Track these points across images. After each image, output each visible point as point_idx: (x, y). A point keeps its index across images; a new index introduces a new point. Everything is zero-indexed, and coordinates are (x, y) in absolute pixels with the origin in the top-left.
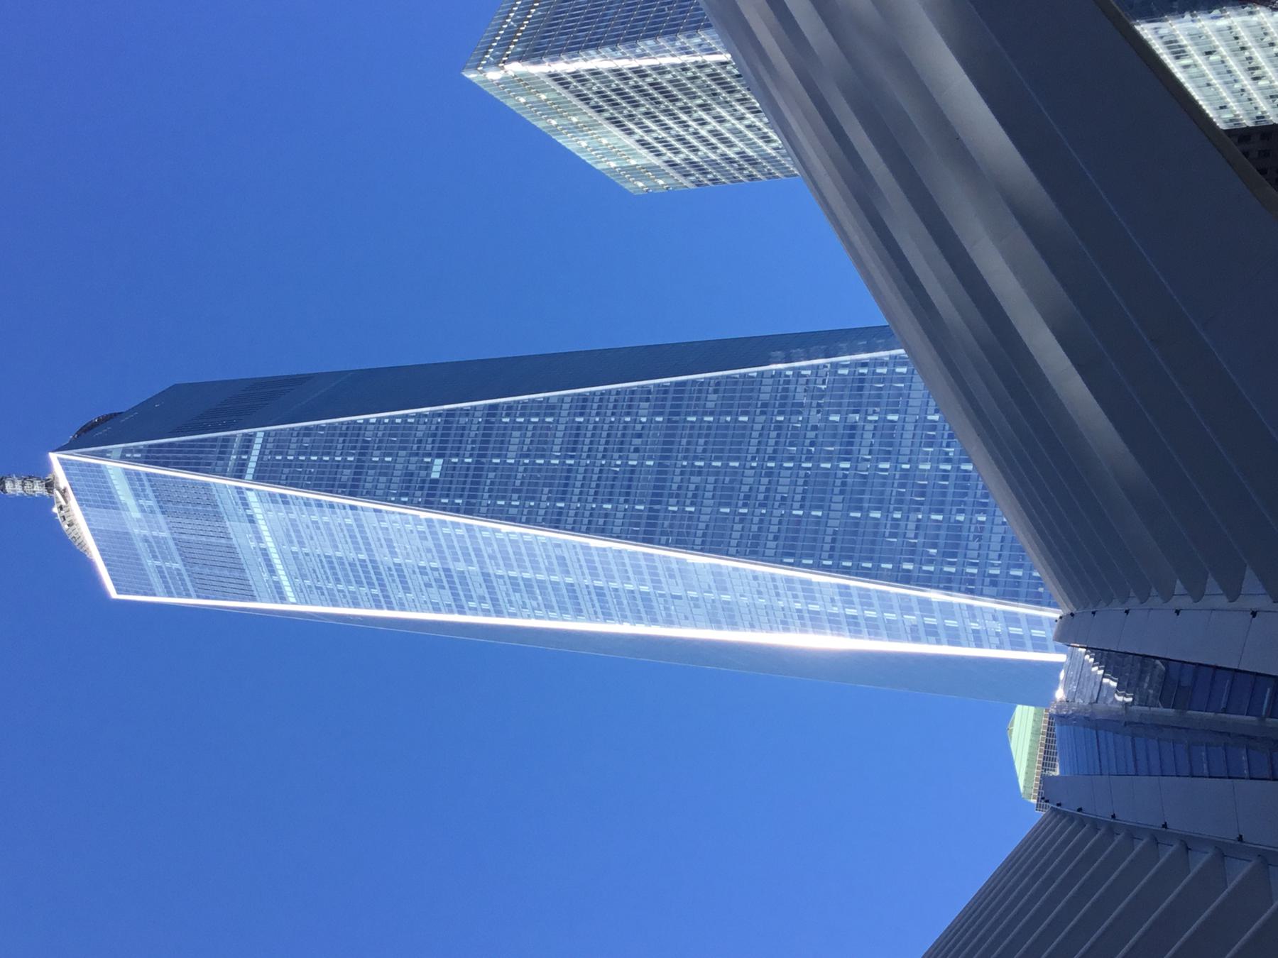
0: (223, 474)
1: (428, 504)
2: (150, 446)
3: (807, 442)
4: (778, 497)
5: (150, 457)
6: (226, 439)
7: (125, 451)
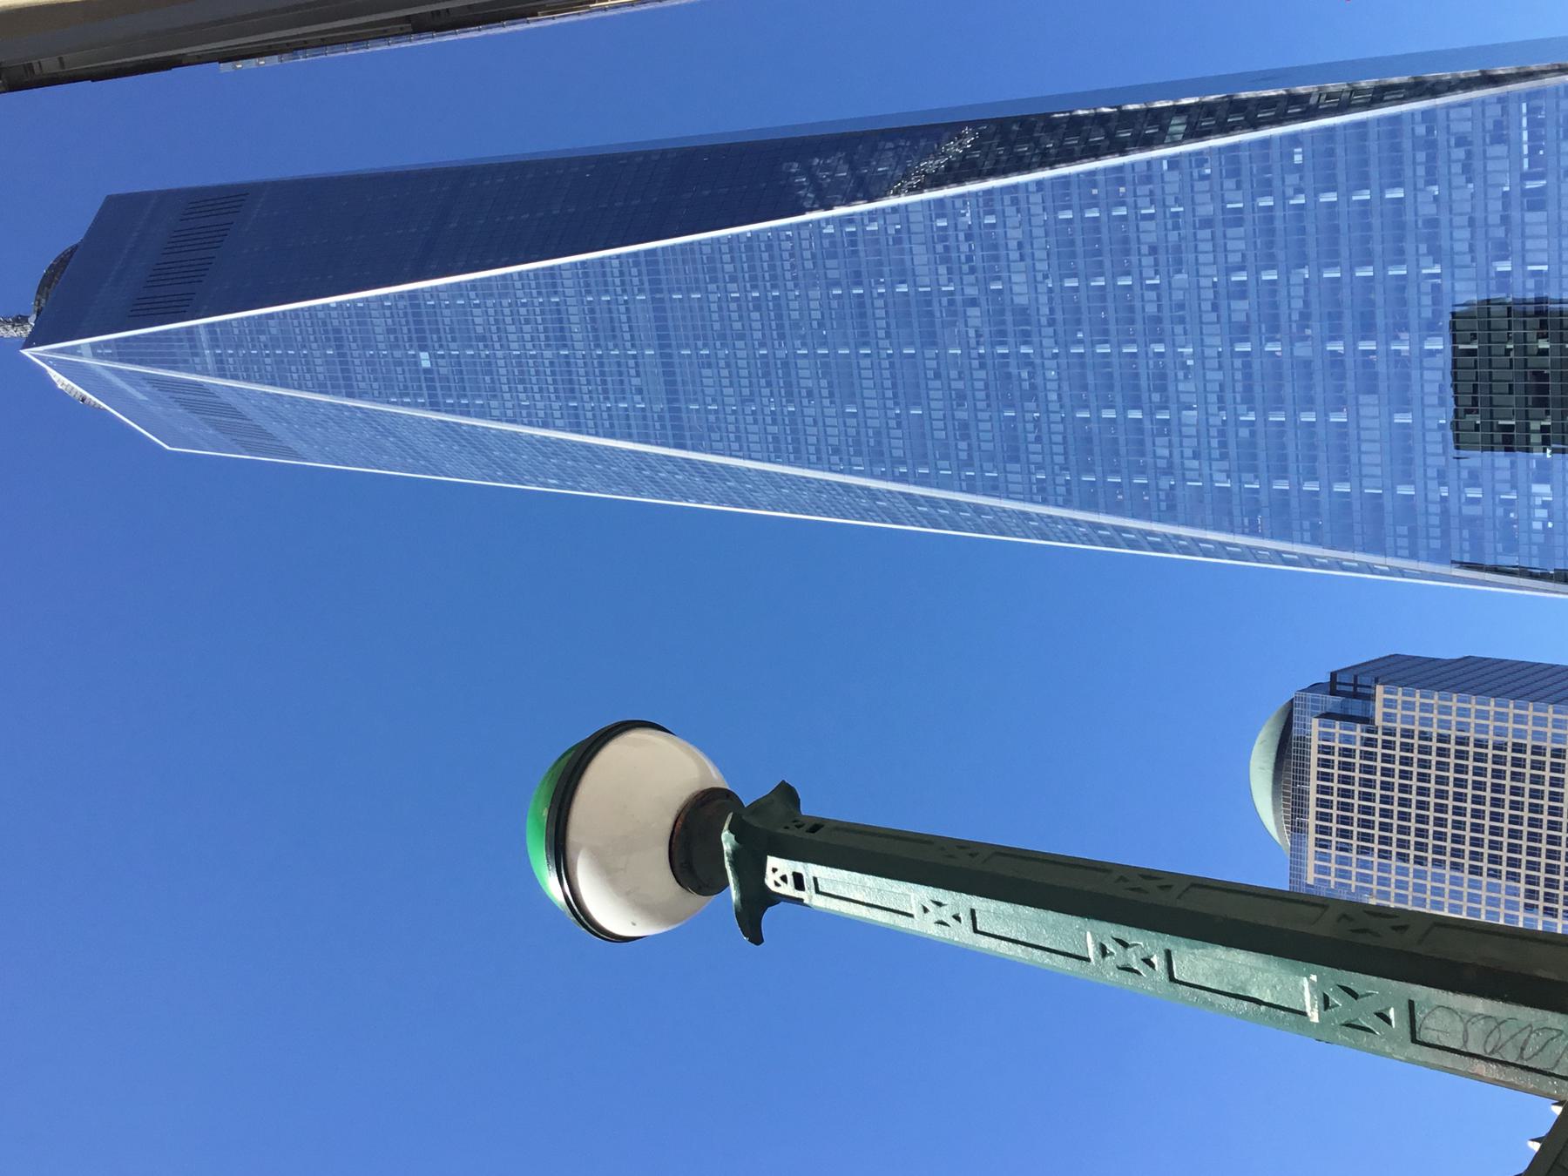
0: (205, 372)
1: (435, 406)
2: (116, 340)
3: (815, 324)
4: (804, 393)
5: (124, 352)
6: (189, 330)
7: (93, 346)
